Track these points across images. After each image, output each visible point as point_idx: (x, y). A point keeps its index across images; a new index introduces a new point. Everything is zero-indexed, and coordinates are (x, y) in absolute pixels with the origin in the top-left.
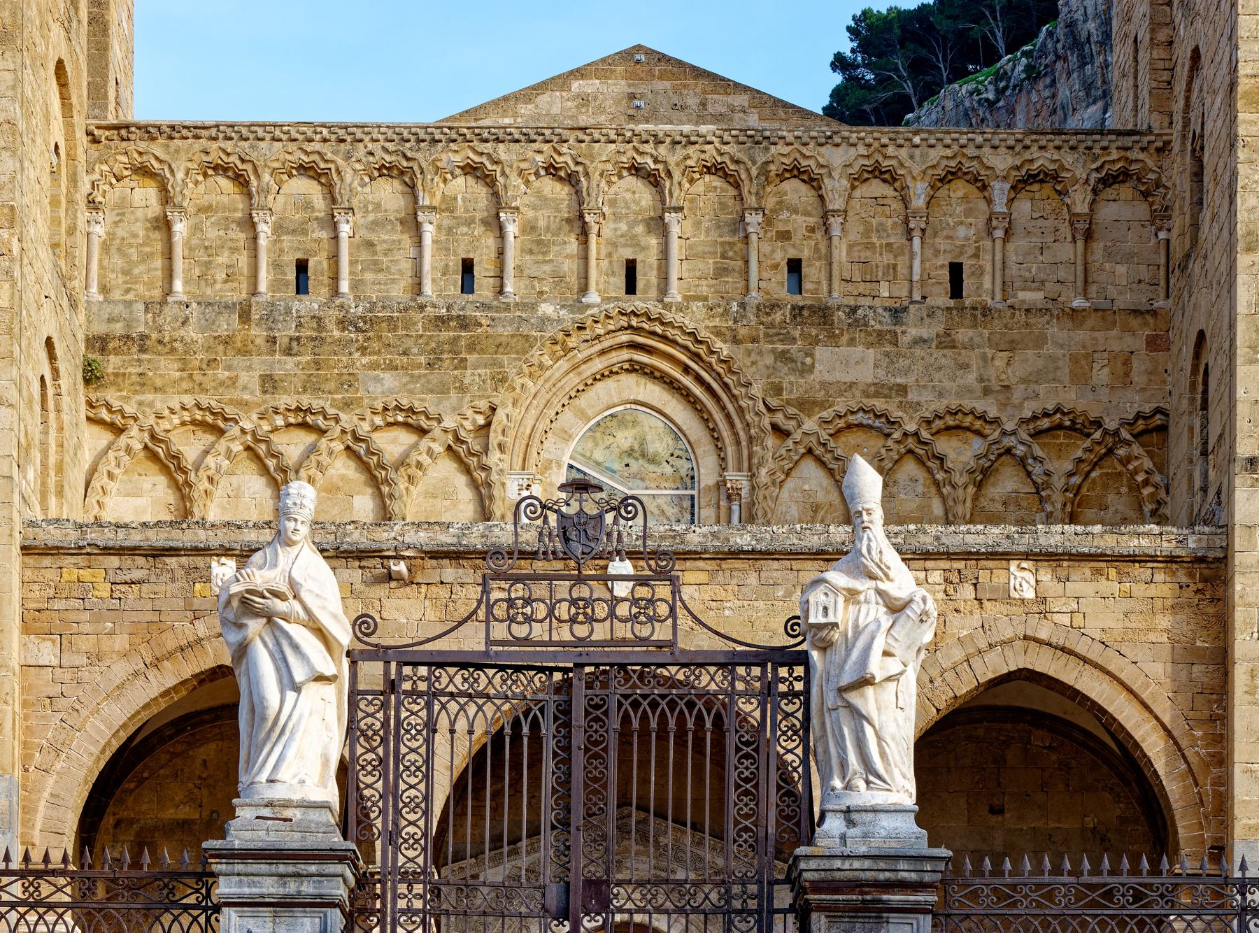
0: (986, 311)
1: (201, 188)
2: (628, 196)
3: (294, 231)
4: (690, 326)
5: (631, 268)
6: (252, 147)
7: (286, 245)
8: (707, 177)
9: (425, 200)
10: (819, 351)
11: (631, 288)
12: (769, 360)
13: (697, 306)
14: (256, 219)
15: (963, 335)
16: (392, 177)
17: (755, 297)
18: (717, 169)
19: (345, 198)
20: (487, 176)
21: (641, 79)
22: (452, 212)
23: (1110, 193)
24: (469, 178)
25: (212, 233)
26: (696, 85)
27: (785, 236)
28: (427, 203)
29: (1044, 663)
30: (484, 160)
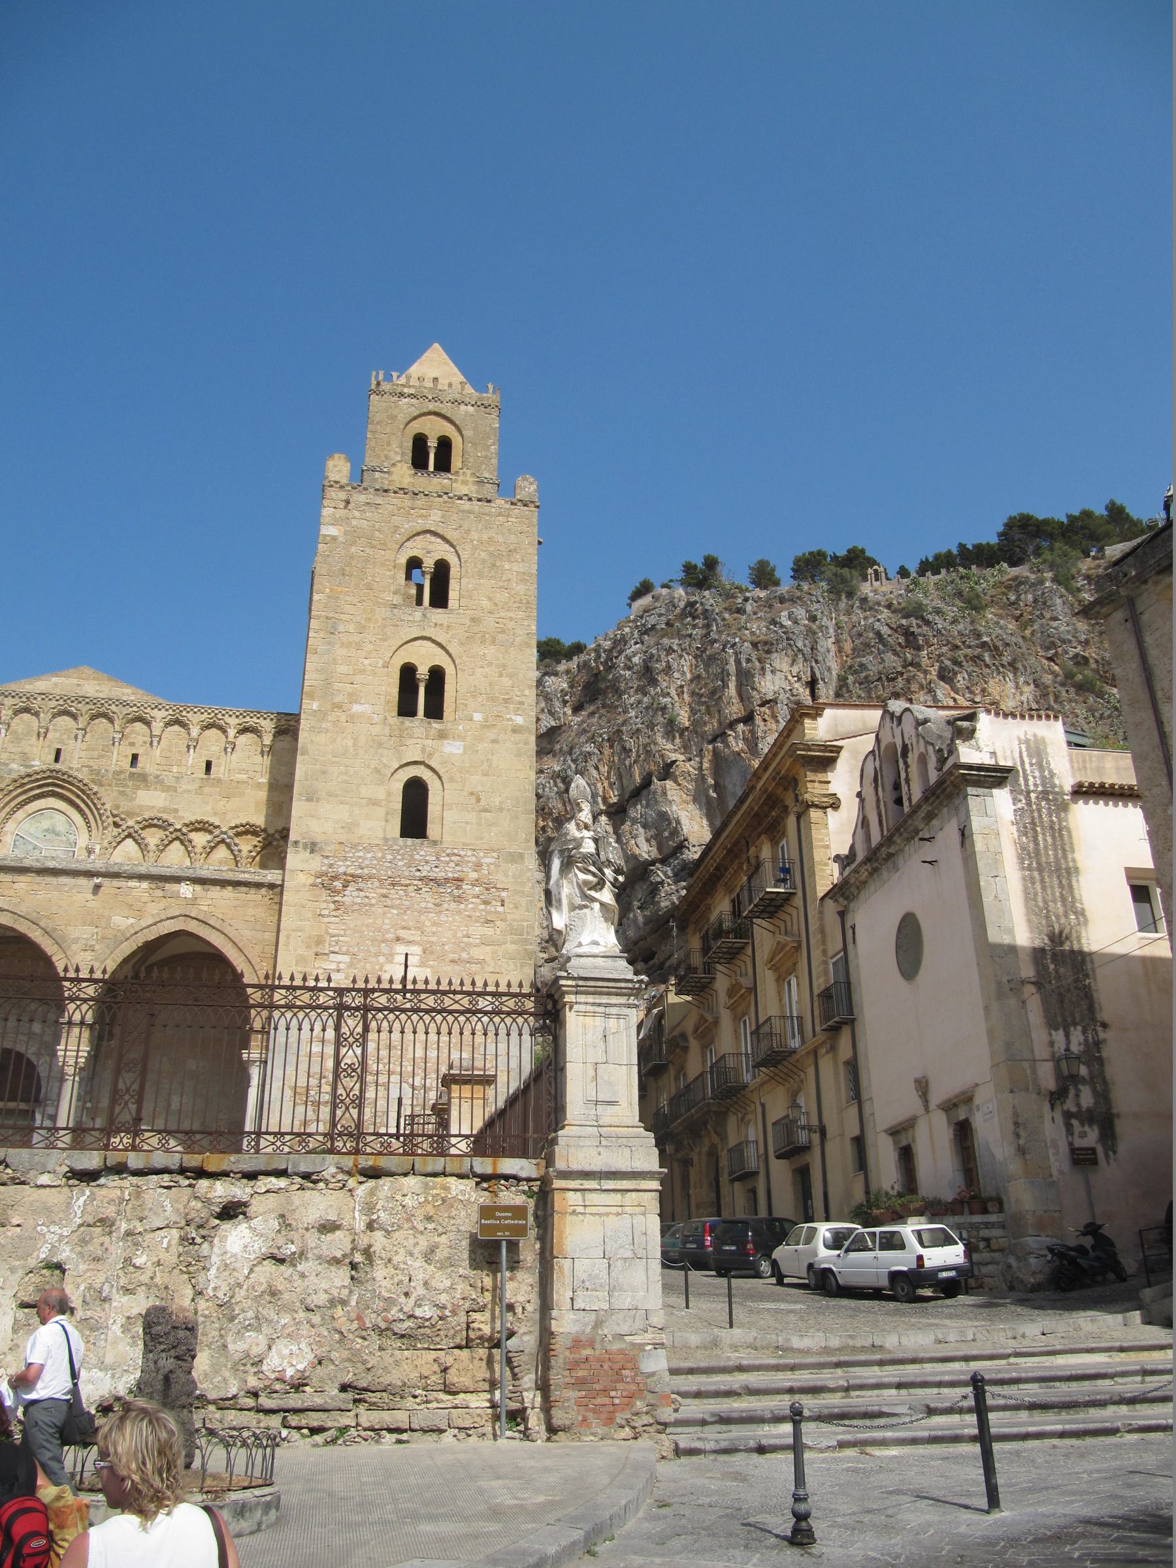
0: (219, 781)
4: (80, 776)
5: (58, 752)
10: (139, 792)
11: (57, 760)
12: (116, 794)
13: (85, 769)
15: (206, 790)
17: (113, 768)
23: (281, 738)
27: (132, 744)
29: (193, 927)
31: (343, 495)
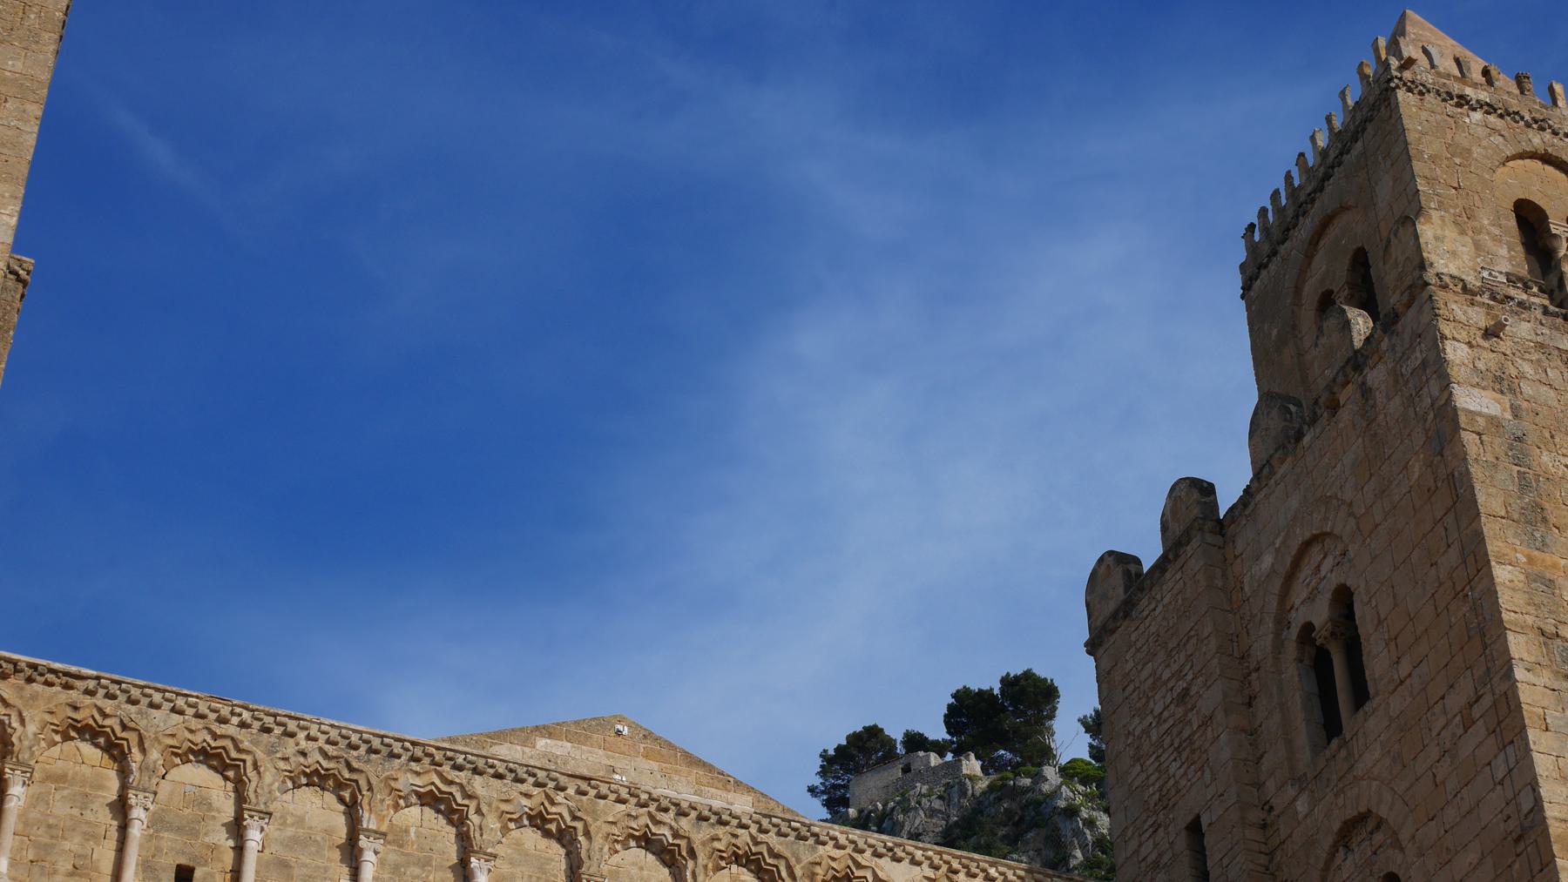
1: (56, 750)
2: (634, 871)
3: (179, 830)
6: (140, 712)
7: (165, 845)
8: (734, 867)
9: (369, 821)
14: (133, 801)
16: (323, 789)
18: (748, 860)
19: (262, 800)
20: (455, 811)
21: (623, 753)
22: (401, 846)
24: (427, 809)
25: (61, 809)
26: (690, 773)
28: (373, 826)
30: (453, 789)
31: (1479, 317)
